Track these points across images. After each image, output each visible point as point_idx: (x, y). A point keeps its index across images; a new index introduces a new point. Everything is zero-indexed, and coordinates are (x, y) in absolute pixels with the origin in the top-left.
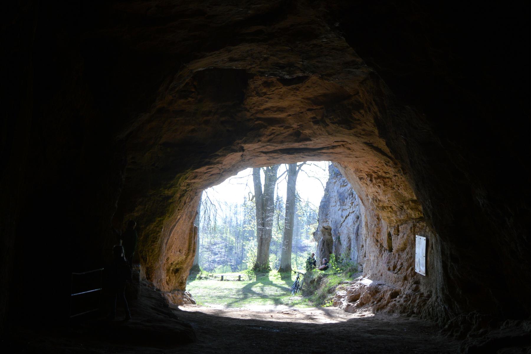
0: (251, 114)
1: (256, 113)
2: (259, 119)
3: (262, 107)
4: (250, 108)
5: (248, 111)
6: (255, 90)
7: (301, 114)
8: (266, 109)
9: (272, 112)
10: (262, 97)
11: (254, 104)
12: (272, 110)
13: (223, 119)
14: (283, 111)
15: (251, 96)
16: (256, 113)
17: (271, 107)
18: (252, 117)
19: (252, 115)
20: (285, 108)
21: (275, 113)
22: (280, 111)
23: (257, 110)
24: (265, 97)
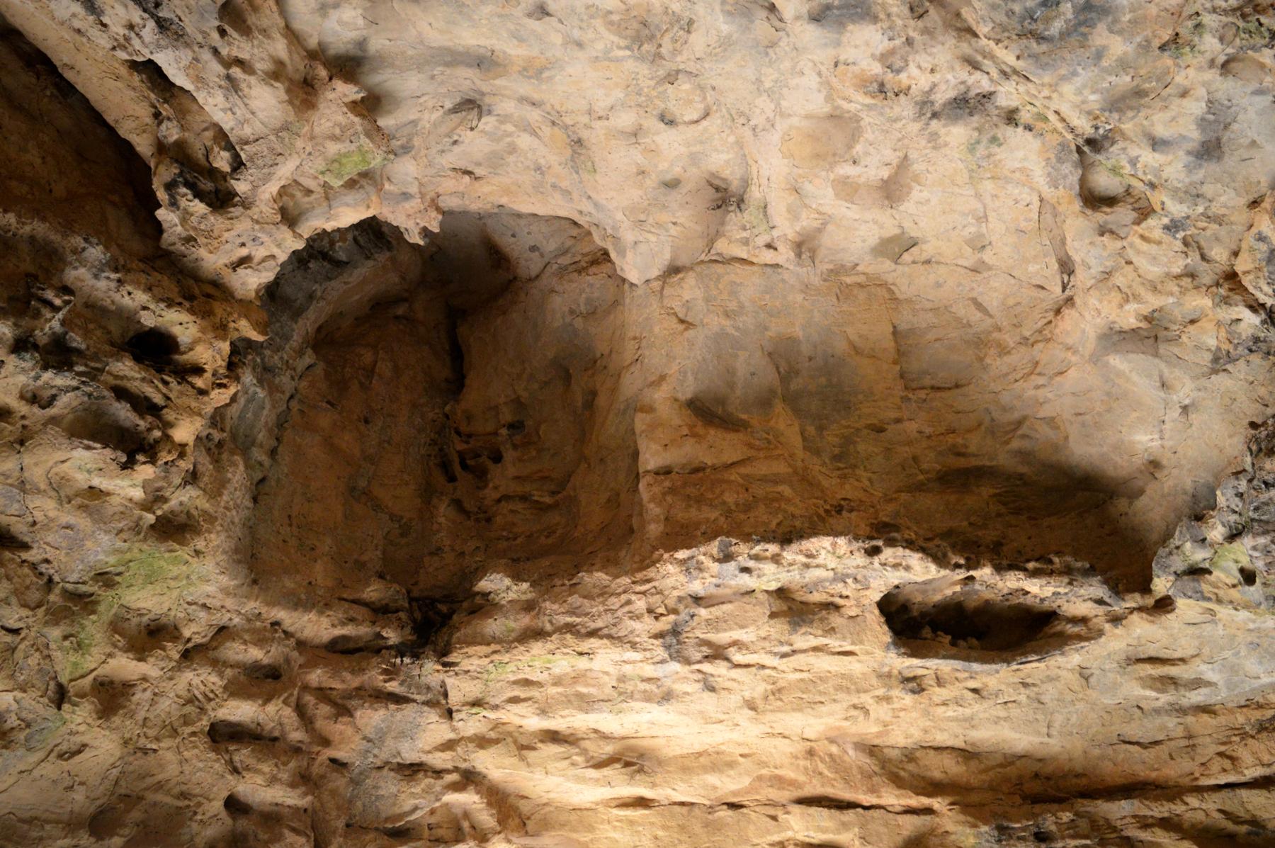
0: (452, 736)
1: (482, 742)
2: (470, 778)
3: (530, 721)
4: (477, 703)
5: (449, 713)
6: (675, 611)
7: (725, 813)
8: (553, 737)
9: (579, 759)
10: (688, 662)
11: (527, 683)
12: (584, 752)
13: (242, 711)
14: (641, 770)
15: (610, 637)
16: (482, 742)
17: (596, 731)
18: (440, 760)
19: (449, 745)
20: (660, 762)
21: (593, 773)
22: (628, 764)
23: (497, 725)
24: (699, 671)
